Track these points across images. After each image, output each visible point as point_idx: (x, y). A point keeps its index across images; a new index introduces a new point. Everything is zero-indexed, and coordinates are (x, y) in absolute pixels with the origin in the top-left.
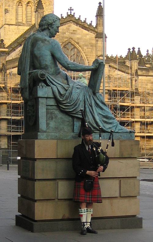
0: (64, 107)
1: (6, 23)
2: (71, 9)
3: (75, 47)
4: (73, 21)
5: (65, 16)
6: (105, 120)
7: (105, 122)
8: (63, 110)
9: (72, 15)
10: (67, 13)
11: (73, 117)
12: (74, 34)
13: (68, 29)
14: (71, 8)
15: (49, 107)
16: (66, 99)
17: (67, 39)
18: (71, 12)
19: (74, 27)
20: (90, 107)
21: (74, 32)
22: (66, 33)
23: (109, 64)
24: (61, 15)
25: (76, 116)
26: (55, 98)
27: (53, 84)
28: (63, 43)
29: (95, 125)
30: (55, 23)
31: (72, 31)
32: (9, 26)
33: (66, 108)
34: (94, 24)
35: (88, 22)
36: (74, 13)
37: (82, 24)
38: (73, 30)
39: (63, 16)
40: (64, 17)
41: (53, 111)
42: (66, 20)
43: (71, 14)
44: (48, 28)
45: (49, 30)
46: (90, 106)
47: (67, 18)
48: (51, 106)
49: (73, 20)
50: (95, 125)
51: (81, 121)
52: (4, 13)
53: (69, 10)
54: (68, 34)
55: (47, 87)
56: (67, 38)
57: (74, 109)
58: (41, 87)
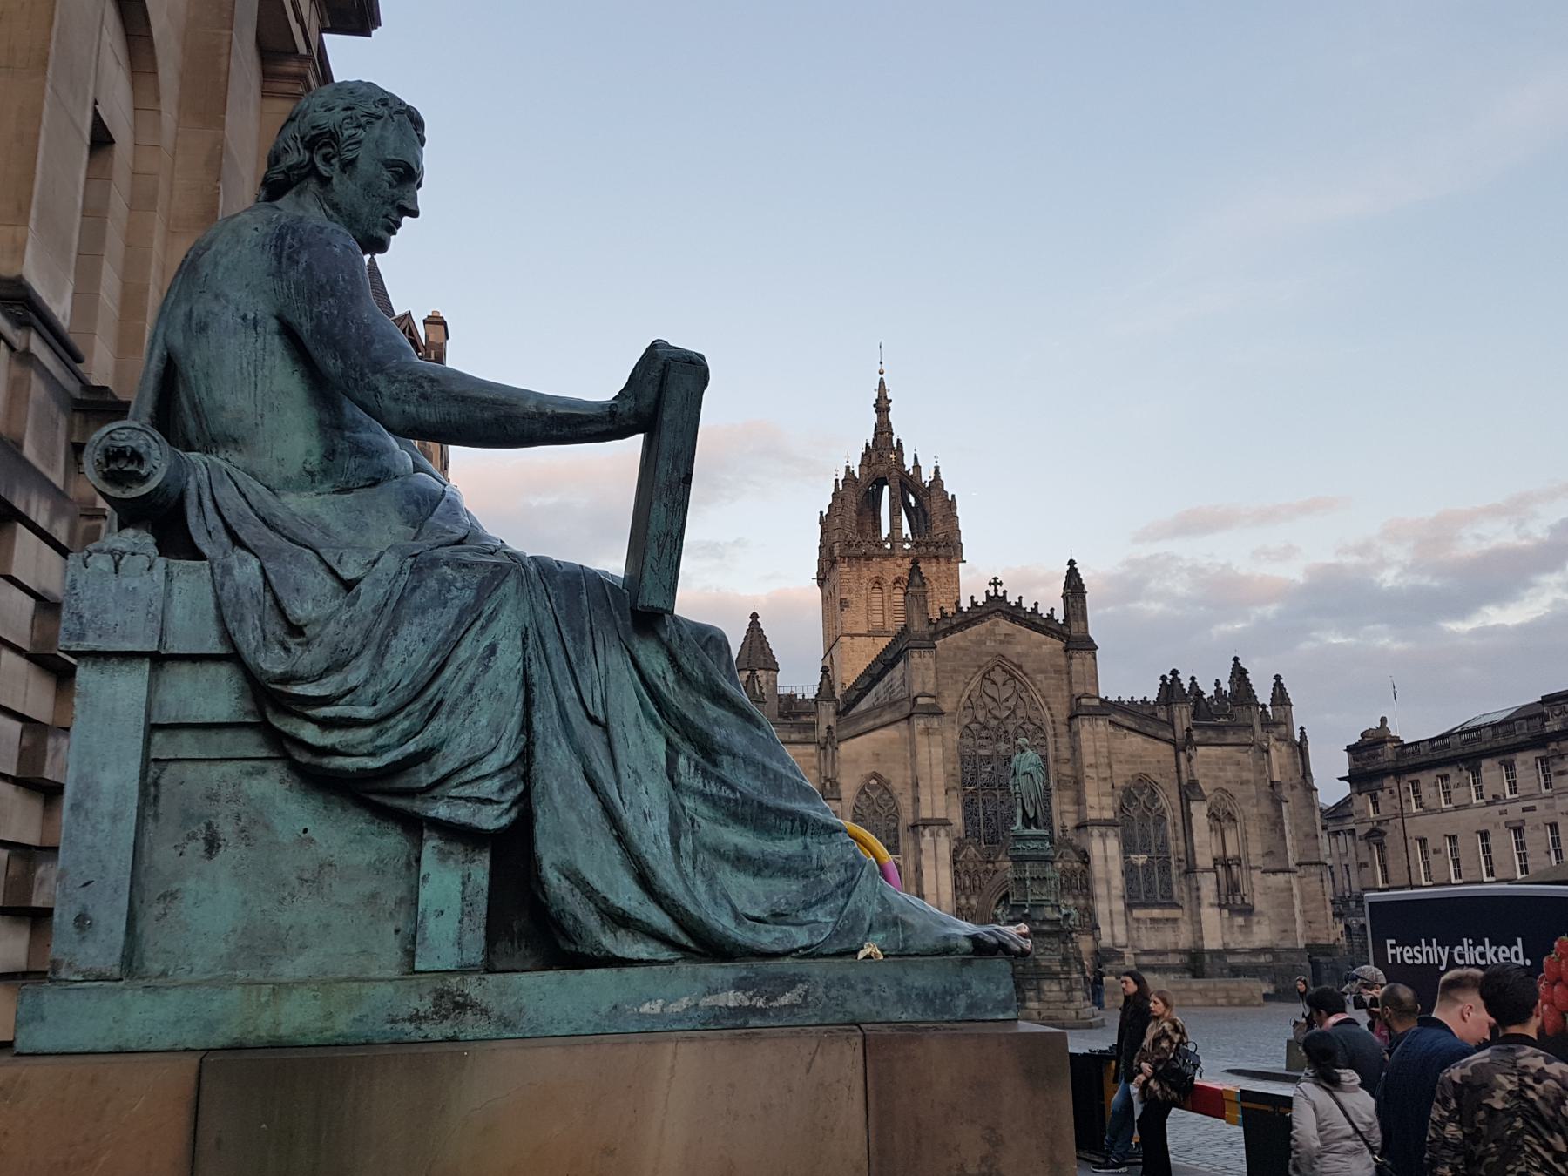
0: (310, 733)
1: (845, 632)
2: (995, 583)
3: (1013, 678)
4: (1002, 612)
5: (981, 599)
6: (737, 838)
7: (740, 861)
8: (308, 764)
9: (1000, 597)
10: (987, 592)
11: (415, 826)
12: (1009, 643)
13: (991, 633)
14: (995, 579)
15: (187, 745)
16: (337, 665)
17: (989, 658)
18: (996, 590)
19: (1004, 626)
20: (593, 739)
21: (1008, 638)
22: (988, 643)
23: (1108, 718)
24: (972, 597)
25: (442, 811)
26: (234, 657)
27: (237, 541)
28: (980, 667)
29: (628, 897)
30: (361, 134)
31: (1002, 638)
32: (852, 639)
33: (333, 738)
34: (1060, 616)
35: (1044, 611)
36: (1005, 592)
37: (1027, 617)
38: (1006, 635)
39: (975, 600)
40: (980, 604)
41: (224, 779)
42: (984, 610)
43: (996, 594)
44: (313, 171)
45: (325, 181)
46: (593, 720)
47: (988, 605)
48: (213, 737)
49: (1004, 609)
50: (628, 897)
51: (488, 849)
52: (838, 608)
53: (990, 584)
54: (993, 644)
55: (161, 562)
56: (989, 654)
57: (411, 747)
58: (103, 563)
